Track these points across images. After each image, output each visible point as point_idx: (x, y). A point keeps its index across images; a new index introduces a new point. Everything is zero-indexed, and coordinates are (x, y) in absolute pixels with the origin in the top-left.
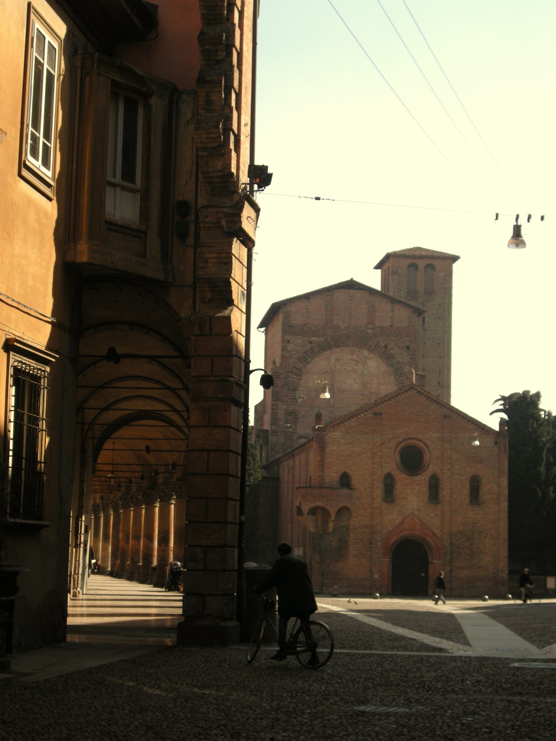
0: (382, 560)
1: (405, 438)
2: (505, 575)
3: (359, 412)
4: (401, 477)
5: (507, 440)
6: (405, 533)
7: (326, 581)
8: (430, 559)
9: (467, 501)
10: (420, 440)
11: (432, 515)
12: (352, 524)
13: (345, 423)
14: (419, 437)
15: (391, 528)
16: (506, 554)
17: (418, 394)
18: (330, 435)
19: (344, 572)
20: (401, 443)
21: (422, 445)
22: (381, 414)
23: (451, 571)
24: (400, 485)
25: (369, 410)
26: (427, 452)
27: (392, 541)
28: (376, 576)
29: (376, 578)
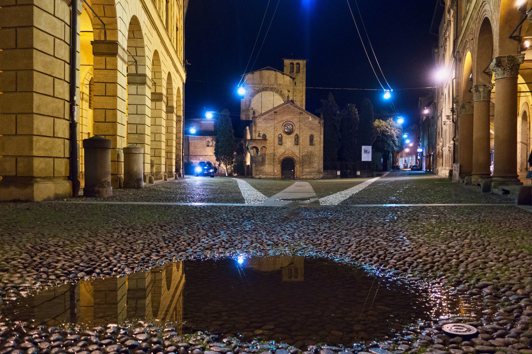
2: (322, 170)
4: (284, 135)
6: (286, 156)
14: (291, 121)
27: (281, 159)
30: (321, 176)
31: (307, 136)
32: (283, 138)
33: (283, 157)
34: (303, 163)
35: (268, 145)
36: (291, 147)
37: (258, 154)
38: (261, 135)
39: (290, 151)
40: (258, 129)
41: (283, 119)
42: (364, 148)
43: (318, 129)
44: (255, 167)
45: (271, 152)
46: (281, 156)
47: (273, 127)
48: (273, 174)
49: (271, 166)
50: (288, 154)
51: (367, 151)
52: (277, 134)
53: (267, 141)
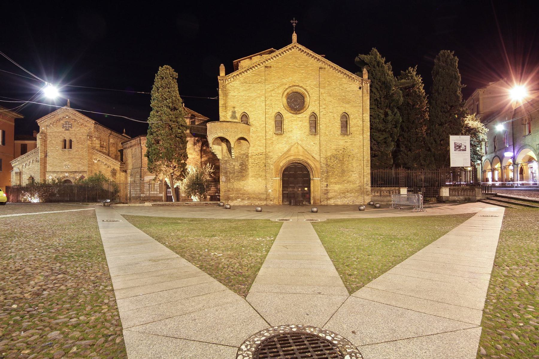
0: (274, 178)
1: (290, 85)
2: (369, 188)
3: (254, 65)
4: (287, 115)
5: (369, 85)
6: (292, 158)
7: (231, 196)
8: (311, 177)
9: (339, 132)
10: (301, 87)
11: (312, 143)
12: (250, 152)
13: (243, 74)
14: (301, 85)
15: (281, 154)
16: (369, 171)
17: (300, 52)
18: (231, 84)
19: (245, 188)
20: (287, 89)
21: (304, 91)
22: (271, 67)
23: (327, 185)
24: (286, 121)
25: (261, 64)
26: (308, 96)
27: (281, 164)
28: (270, 191)
29: (270, 192)
30: (368, 199)
31: (335, 115)
32: (286, 122)
33: (284, 162)
34: (327, 172)
35: (254, 135)
36: (302, 140)
37: (231, 154)
38: (238, 115)
39: (300, 147)
40: (230, 103)
41: (284, 81)
42: (453, 139)
43: (359, 100)
44: (225, 182)
45: (259, 151)
46: (280, 158)
47: (263, 98)
48: (264, 197)
49: (260, 179)
50: (297, 155)
51: (460, 147)
52: (272, 113)
53: (252, 129)
